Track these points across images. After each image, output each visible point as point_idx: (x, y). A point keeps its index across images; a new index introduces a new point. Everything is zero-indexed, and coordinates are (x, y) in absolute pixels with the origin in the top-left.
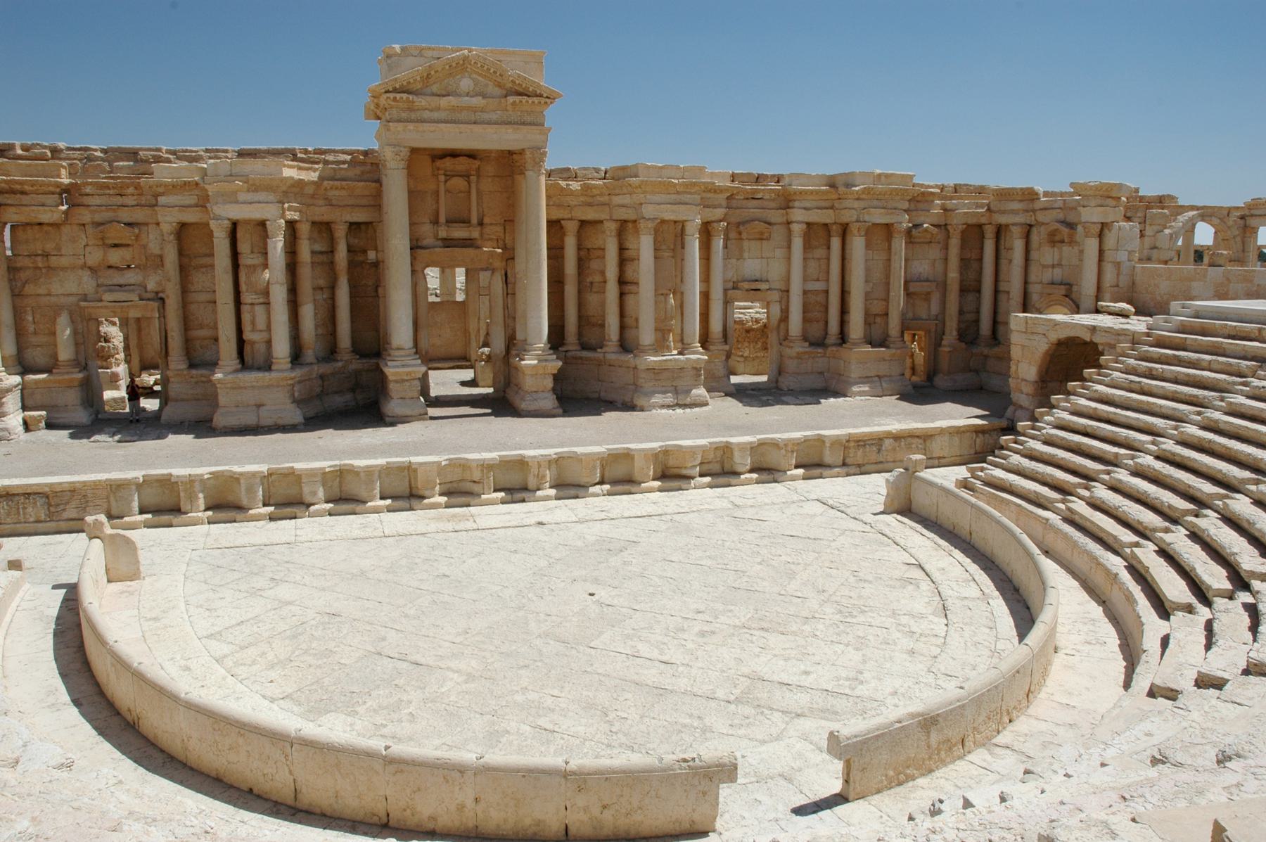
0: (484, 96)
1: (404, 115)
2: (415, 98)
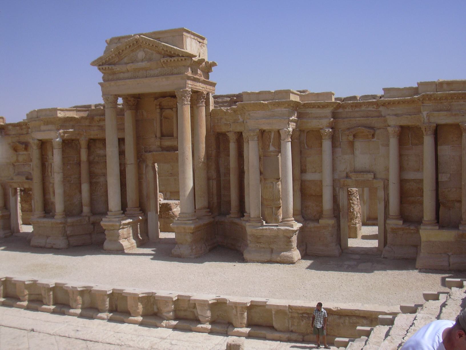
0: (150, 60)
1: (110, 77)
2: (113, 67)
